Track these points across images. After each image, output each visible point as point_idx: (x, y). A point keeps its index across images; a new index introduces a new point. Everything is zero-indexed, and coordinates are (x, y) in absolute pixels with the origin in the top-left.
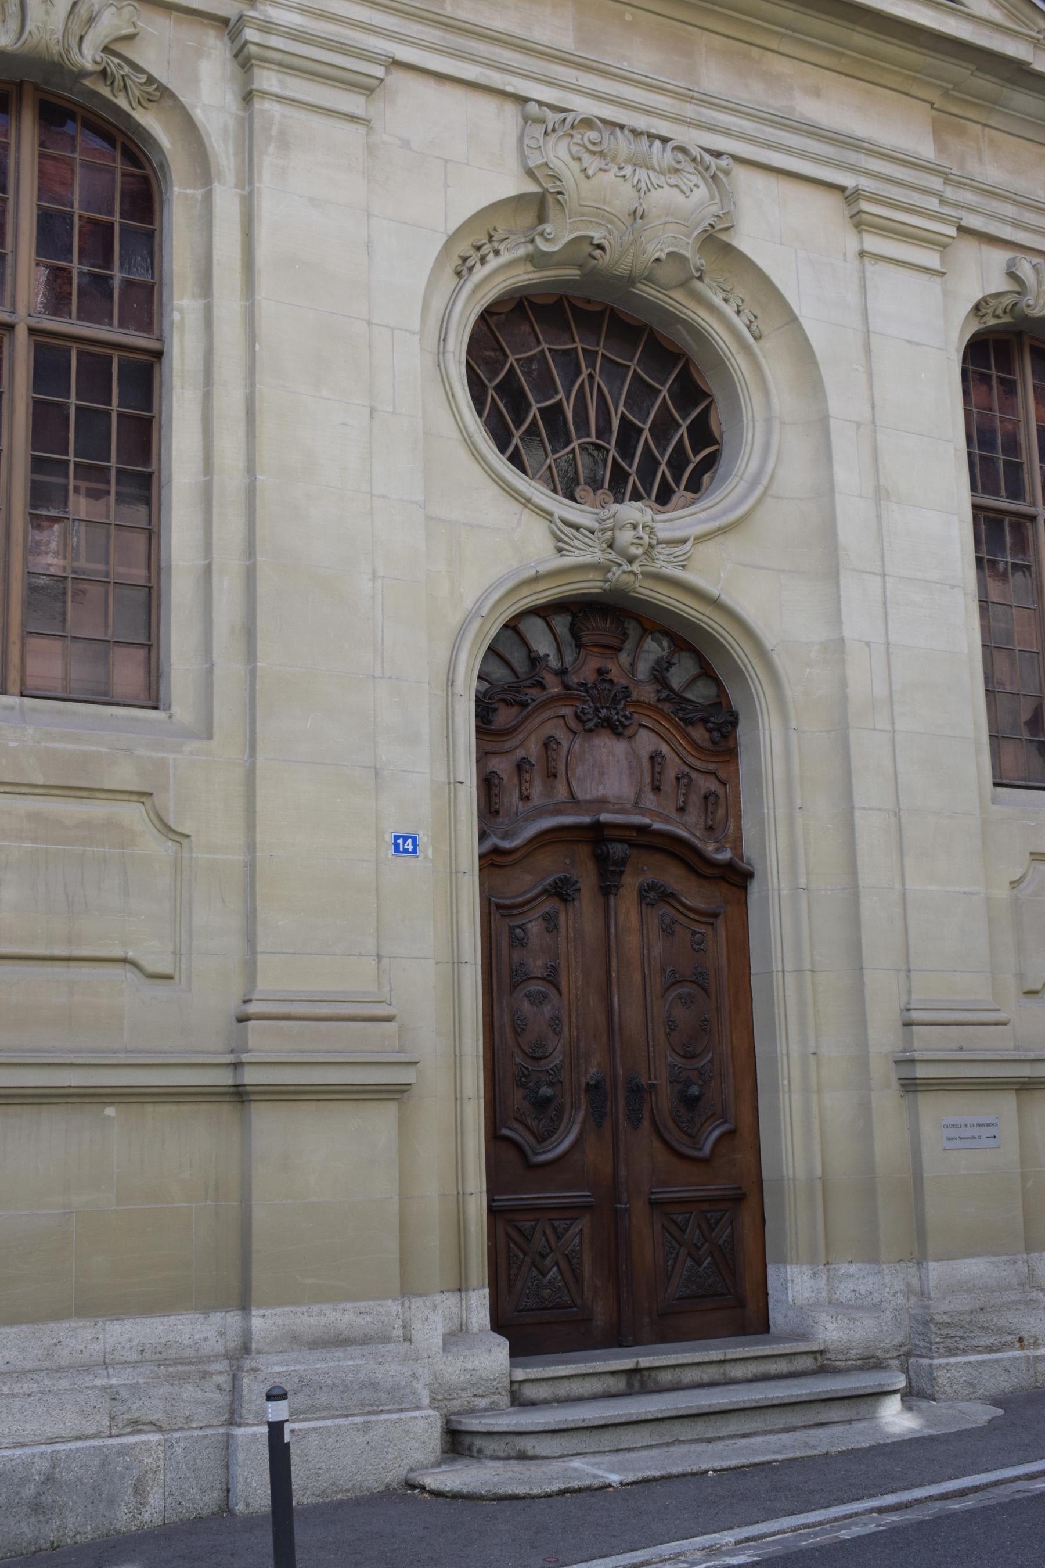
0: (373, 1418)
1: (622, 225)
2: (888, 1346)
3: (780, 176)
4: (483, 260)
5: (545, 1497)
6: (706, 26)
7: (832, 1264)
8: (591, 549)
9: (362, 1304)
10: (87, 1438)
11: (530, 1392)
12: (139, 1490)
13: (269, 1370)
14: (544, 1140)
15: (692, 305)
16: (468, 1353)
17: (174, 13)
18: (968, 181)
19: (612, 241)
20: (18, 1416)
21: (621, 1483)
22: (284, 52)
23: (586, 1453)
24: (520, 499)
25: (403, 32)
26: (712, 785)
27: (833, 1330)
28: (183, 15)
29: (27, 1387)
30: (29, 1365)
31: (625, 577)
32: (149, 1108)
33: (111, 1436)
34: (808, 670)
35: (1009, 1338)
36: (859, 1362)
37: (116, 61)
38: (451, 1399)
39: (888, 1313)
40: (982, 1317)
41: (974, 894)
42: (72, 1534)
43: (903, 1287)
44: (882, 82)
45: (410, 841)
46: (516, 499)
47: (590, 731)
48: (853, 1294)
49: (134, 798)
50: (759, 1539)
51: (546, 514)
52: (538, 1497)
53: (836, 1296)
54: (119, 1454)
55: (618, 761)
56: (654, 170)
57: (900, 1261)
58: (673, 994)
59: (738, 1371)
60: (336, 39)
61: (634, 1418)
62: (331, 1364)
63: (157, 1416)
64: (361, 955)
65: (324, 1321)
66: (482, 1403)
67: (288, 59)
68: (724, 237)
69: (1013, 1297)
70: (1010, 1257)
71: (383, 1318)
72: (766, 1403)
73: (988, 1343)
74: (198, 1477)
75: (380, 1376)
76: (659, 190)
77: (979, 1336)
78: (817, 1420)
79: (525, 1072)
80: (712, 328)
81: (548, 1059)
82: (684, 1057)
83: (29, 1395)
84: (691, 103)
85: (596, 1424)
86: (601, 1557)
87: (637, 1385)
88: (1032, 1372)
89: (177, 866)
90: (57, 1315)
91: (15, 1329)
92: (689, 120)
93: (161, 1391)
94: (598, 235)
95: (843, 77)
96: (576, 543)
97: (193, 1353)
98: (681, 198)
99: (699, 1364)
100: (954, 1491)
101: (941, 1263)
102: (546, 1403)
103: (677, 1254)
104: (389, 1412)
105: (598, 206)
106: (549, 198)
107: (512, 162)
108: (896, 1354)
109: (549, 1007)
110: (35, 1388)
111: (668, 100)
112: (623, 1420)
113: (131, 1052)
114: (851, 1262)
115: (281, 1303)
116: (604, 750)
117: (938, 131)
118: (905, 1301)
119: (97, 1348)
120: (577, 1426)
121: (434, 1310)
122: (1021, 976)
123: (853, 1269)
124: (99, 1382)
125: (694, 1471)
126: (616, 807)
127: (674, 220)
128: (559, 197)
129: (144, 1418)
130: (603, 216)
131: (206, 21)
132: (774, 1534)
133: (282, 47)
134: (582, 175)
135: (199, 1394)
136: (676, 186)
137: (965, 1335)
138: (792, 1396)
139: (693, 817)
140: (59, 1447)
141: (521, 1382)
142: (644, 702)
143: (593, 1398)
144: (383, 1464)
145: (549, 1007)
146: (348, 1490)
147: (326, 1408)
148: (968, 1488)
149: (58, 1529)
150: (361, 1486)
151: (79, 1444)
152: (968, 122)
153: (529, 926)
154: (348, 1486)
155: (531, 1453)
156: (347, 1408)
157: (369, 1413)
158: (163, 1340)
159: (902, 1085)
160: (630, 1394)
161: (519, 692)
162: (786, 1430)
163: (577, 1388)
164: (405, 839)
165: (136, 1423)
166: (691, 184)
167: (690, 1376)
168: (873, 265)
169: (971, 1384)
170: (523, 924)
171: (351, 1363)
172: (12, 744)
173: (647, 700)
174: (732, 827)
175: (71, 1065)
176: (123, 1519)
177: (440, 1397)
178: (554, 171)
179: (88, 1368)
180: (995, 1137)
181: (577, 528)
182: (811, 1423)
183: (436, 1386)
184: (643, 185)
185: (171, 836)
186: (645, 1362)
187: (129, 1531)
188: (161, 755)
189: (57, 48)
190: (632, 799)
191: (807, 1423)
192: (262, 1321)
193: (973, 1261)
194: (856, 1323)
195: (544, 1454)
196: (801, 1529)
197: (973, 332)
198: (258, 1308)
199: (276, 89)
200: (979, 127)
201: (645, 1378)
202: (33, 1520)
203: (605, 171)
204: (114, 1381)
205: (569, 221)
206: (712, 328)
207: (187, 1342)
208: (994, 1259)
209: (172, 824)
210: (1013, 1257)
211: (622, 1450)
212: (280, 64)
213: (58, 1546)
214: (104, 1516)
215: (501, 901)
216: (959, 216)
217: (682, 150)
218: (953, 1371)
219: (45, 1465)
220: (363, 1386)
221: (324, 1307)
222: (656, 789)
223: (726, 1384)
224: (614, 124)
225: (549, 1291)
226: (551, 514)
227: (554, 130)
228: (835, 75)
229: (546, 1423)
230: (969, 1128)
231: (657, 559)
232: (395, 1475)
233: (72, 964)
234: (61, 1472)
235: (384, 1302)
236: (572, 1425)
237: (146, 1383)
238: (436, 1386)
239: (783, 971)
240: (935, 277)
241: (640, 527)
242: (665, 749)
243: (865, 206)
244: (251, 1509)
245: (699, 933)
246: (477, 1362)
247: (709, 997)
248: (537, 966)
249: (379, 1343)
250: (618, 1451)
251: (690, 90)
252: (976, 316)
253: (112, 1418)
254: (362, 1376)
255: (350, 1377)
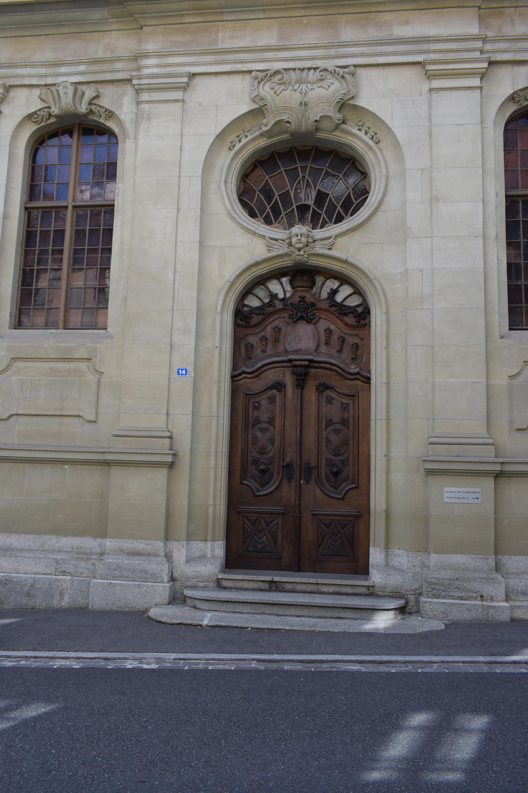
0: (143, 583)
1: (297, 110)
2: (409, 589)
3: (385, 67)
4: (240, 141)
5: (171, 624)
6: (292, 15)
7: (391, 549)
8: (283, 248)
9: (148, 542)
10: (48, 574)
11: (224, 583)
12: (61, 594)
13: (107, 561)
14: (264, 486)
15: (345, 136)
16: (196, 565)
17: (115, 83)
18: (500, 38)
19: (293, 118)
20: (26, 564)
21: (206, 625)
22: (147, 84)
23: (220, 611)
24: (252, 233)
25: (198, 61)
26: (356, 340)
27: (378, 578)
28: (119, 83)
29: (31, 555)
30: (36, 548)
31: (297, 257)
32: (80, 466)
33: (55, 575)
34: (395, 286)
35: (474, 595)
36: (391, 594)
37: (94, 106)
38: (188, 581)
39: (409, 574)
40: (457, 583)
41: (479, 383)
42: (38, 605)
43: (419, 563)
44: (446, 6)
45: (184, 370)
46: (251, 233)
47: (296, 322)
48: (399, 563)
49: (86, 360)
50: (187, 660)
51: (263, 237)
52: (169, 624)
53: (392, 563)
54: (55, 581)
55: (308, 334)
56: (310, 83)
57: (419, 551)
58: (330, 428)
59: (325, 589)
60: (166, 73)
61: (241, 601)
62: (130, 562)
63: (71, 571)
64: (160, 414)
65: (133, 546)
66: (202, 585)
67: (150, 86)
68: (351, 102)
69: (480, 576)
70: (484, 556)
71: (156, 548)
72: (308, 604)
73: (460, 595)
74: (81, 594)
75: (148, 568)
76: (313, 91)
77: (455, 592)
78: (338, 616)
79: (256, 459)
80: (356, 144)
81: (267, 455)
82: (334, 455)
83: (30, 558)
84: (333, 48)
85: (223, 600)
86: (120, 652)
87: (274, 588)
88: (485, 613)
89: (99, 383)
90: (46, 533)
91: (32, 536)
92: (332, 56)
93: (73, 563)
94: (285, 117)
95: (423, 11)
96: (276, 246)
97: (89, 551)
98: (324, 91)
99: (305, 583)
100: (308, 660)
101: (438, 555)
102: (230, 589)
103: (324, 537)
104: (151, 582)
105: (284, 105)
106: (263, 108)
107: (247, 99)
108: (412, 593)
109: (269, 434)
110: (33, 555)
111: (321, 51)
112: (236, 600)
113: (79, 447)
114: (399, 549)
115: (118, 538)
116: (301, 330)
117: (481, 20)
118: (420, 570)
119: (58, 545)
120: (214, 599)
121: (183, 547)
122: (511, 422)
123: (400, 552)
124: (53, 557)
125: (242, 626)
126: (306, 352)
127: (321, 102)
128: (266, 107)
129: (66, 571)
130: (287, 109)
131: (127, 82)
132: (195, 659)
133: (146, 83)
134: (275, 95)
135: (86, 566)
136: (321, 87)
137: (446, 590)
138: (323, 603)
139: (347, 354)
140: (37, 576)
141: (222, 579)
142: (323, 309)
143: (253, 590)
144: (145, 601)
145: (269, 434)
146: (130, 608)
147: (126, 577)
148: (317, 660)
149: (34, 602)
150: (135, 607)
151: (43, 576)
152: (505, 9)
153: (262, 402)
154: (131, 606)
155: (197, 607)
156: (134, 578)
157: (143, 581)
158: (80, 546)
159: (426, 472)
160: (270, 591)
161: (262, 310)
162: (320, 617)
163: (245, 585)
164: (182, 370)
165: (64, 572)
166: (329, 84)
167: (300, 587)
168: (437, 94)
169: (445, 613)
170: (259, 401)
171: (138, 562)
172: (46, 345)
173: (324, 308)
174: (365, 358)
175: (50, 451)
176: (55, 603)
177: (183, 580)
178: (261, 97)
179: (53, 552)
180: (478, 498)
181: (276, 240)
182: (335, 616)
183: (182, 575)
184: (304, 91)
185: (98, 373)
186: (276, 579)
187: (57, 607)
188: (95, 345)
189: (72, 108)
190: (314, 349)
191: (332, 616)
192: (110, 543)
193: (459, 556)
194: (390, 576)
195: (202, 608)
196: (211, 660)
197: (513, 111)
198: (109, 538)
199: (147, 99)
200: (513, 9)
201: (278, 585)
202: (26, 598)
203: (285, 90)
204: (58, 557)
205: (272, 115)
206: (356, 144)
207: (88, 547)
208: (473, 556)
209: (97, 369)
210: (486, 556)
211: (237, 612)
212: (148, 89)
213: (34, 608)
214: (49, 601)
215: (248, 392)
216: (489, 56)
217: (326, 70)
218: (434, 605)
219: (30, 581)
220: (141, 571)
221: (134, 541)
222: (327, 344)
223: (318, 593)
224: (289, 69)
225: (261, 545)
226: (265, 237)
227: (262, 80)
228: (419, 11)
229: (202, 596)
230: (461, 493)
231: (315, 247)
232: (140, 605)
233: (62, 417)
234: (36, 584)
235: (157, 542)
236: (212, 599)
237: (68, 559)
238: (182, 575)
239: (376, 419)
240: (476, 90)
241: (299, 235)
242: (332, 327)
243: (429, 67)
244: (93, 608)
245: (345, 403)
246: (199, 569)
247: (349, 430)
248: (264, 417)
249: (153, 556)
250: (235, 612)
251: (331, 43)
252: (515, 102)
253: (56, 569)
254: (141, 567)
255: (136, 567)
